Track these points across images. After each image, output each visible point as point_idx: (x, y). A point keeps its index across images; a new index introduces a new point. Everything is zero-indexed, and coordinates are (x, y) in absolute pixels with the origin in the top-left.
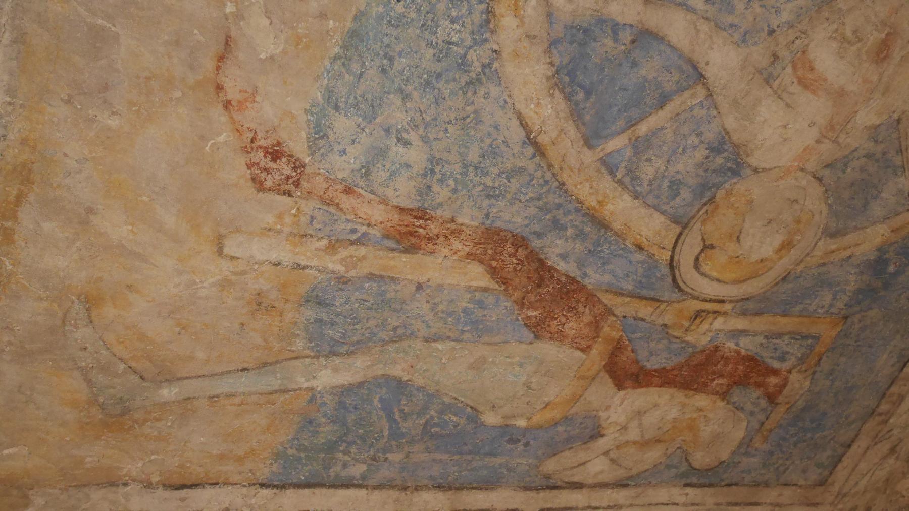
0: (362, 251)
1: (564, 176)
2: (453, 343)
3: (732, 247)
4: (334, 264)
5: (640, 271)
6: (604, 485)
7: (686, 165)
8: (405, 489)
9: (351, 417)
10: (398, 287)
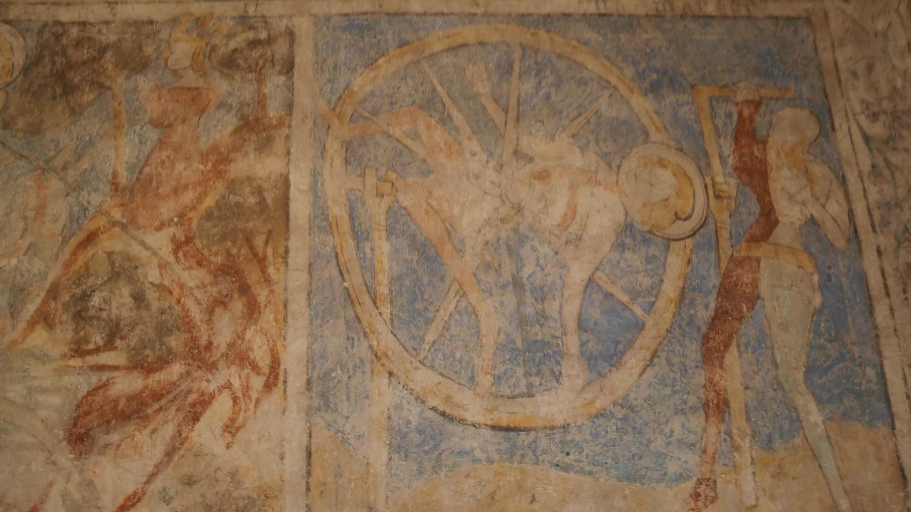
0: (735, 431)
1: (663, 332)
2: (775, 350)
3: (672, 201)
4: (746, 444)
5: (702, 253)
6: (847, 195)
7: (634, 259)
8: (877, 336)
9: (836, 391)
10: (750, 400)
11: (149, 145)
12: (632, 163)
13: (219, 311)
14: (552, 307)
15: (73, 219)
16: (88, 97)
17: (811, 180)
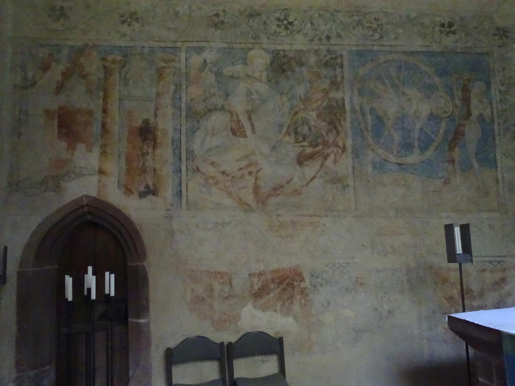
4: (458, 170)
13: (330, 133)
15: (292, 108)
16: (290, 73)
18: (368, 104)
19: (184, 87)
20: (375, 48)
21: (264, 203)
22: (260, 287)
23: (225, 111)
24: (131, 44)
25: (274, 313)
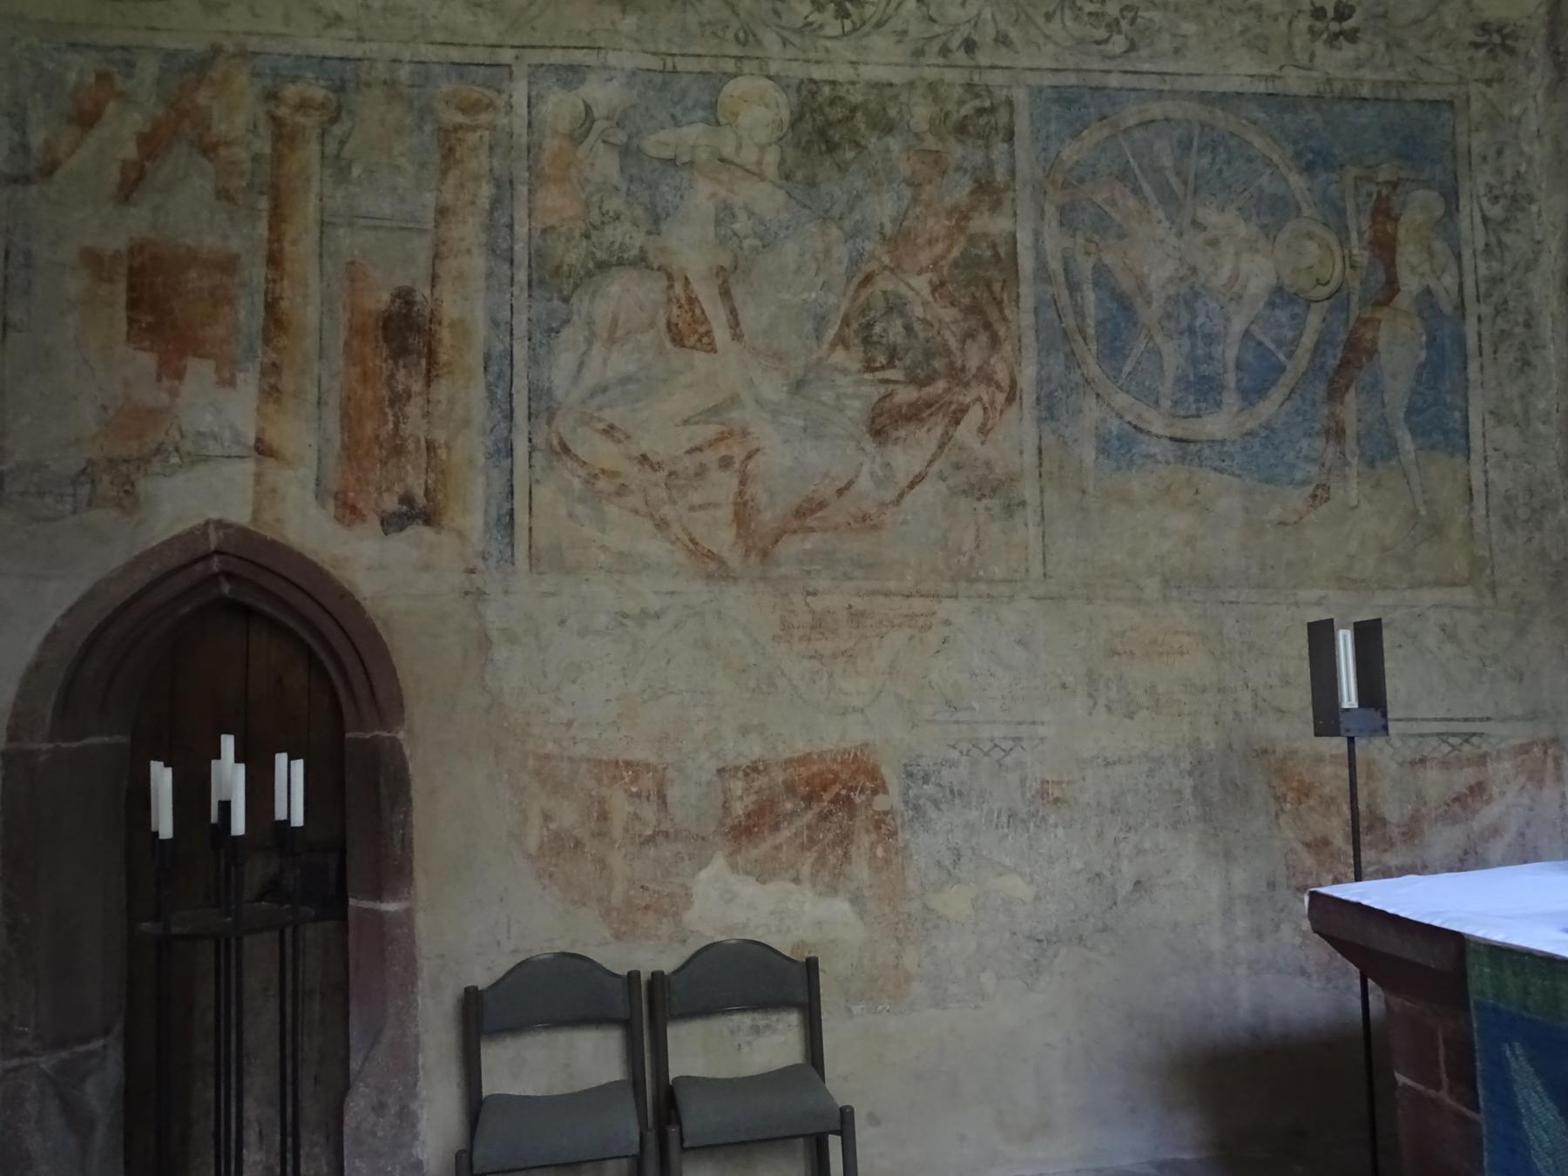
4: (1355, 461)
6: (1460, 267)
7: (1282, 315)
11: (906, 202)
12: (1284, 236)
13: (969, 342)
14: (1217, 351)
17: (1431, 255)
18: (1088, 254)
19: (523, 190)
20: (1114, 81)
21: (765, 554)
22: (751, 807)
23: (649, 267)
24: (357, 51)
25: (792, 886)
